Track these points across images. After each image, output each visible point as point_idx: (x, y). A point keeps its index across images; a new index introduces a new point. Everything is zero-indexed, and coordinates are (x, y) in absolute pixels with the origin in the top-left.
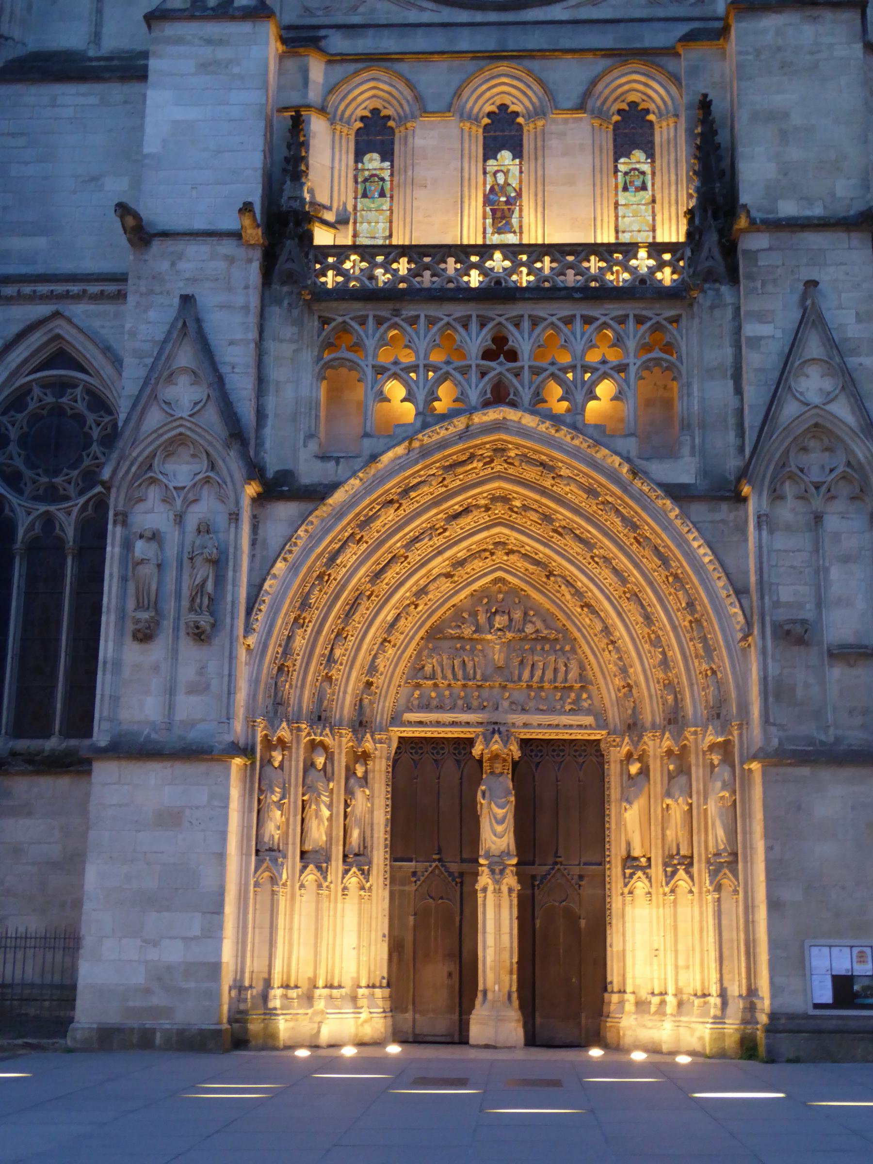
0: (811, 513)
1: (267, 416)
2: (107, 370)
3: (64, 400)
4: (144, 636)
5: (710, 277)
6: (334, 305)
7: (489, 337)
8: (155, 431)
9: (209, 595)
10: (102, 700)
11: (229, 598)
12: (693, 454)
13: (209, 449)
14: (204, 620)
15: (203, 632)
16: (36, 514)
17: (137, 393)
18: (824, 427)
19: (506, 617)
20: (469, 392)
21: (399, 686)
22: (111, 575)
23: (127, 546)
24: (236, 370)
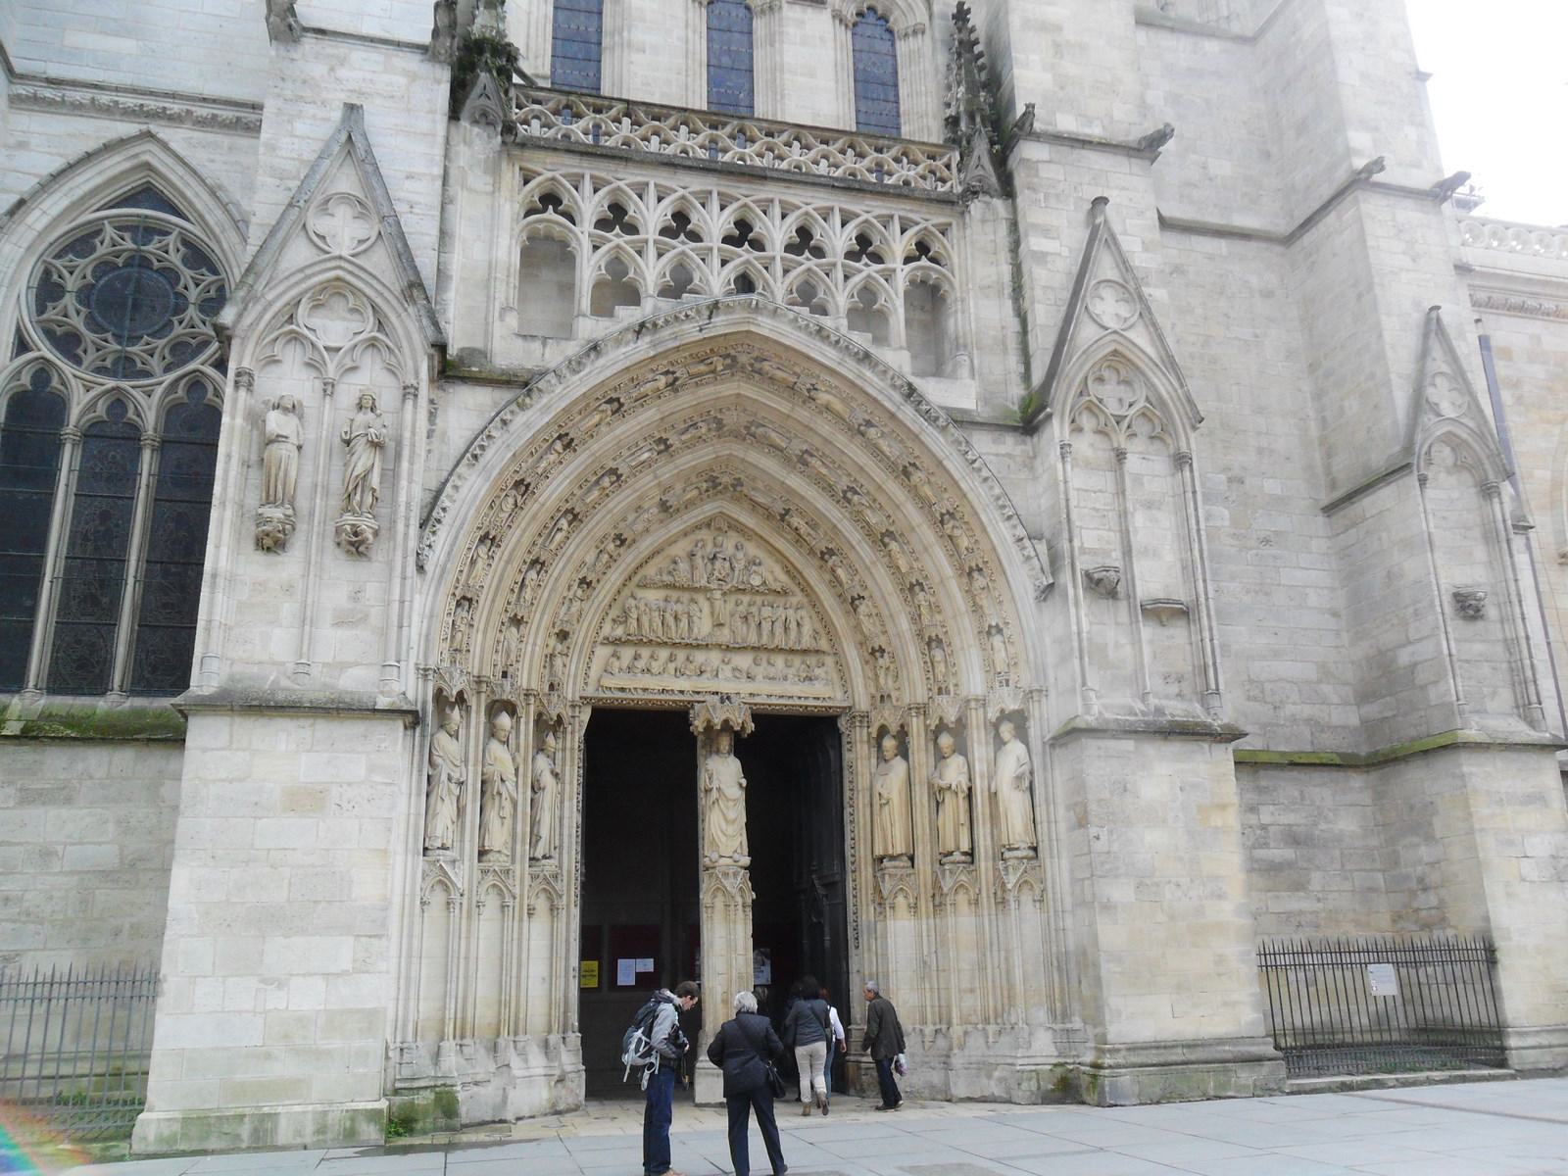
0: (1113, 449)
1: (451, 277)
2: (215, 217)
3: (150, 248)
4: (271, 543)
6: (540, 155)
7: (732, 220)
8: (301, 270)
9: (374, 490)
10: (208, 630)
11: (402, 498)
12: (973, 376)
13: (379, 301)
14: (366, 525)
15: (362, 542)
16: (100, 389)
17: (274, 223)
18: (1124, 356)
19: (727, 564)
20: (711, 278)
21: (595, 642)
22: (229, 456)
23: (256, 420)
24: (415, 210)
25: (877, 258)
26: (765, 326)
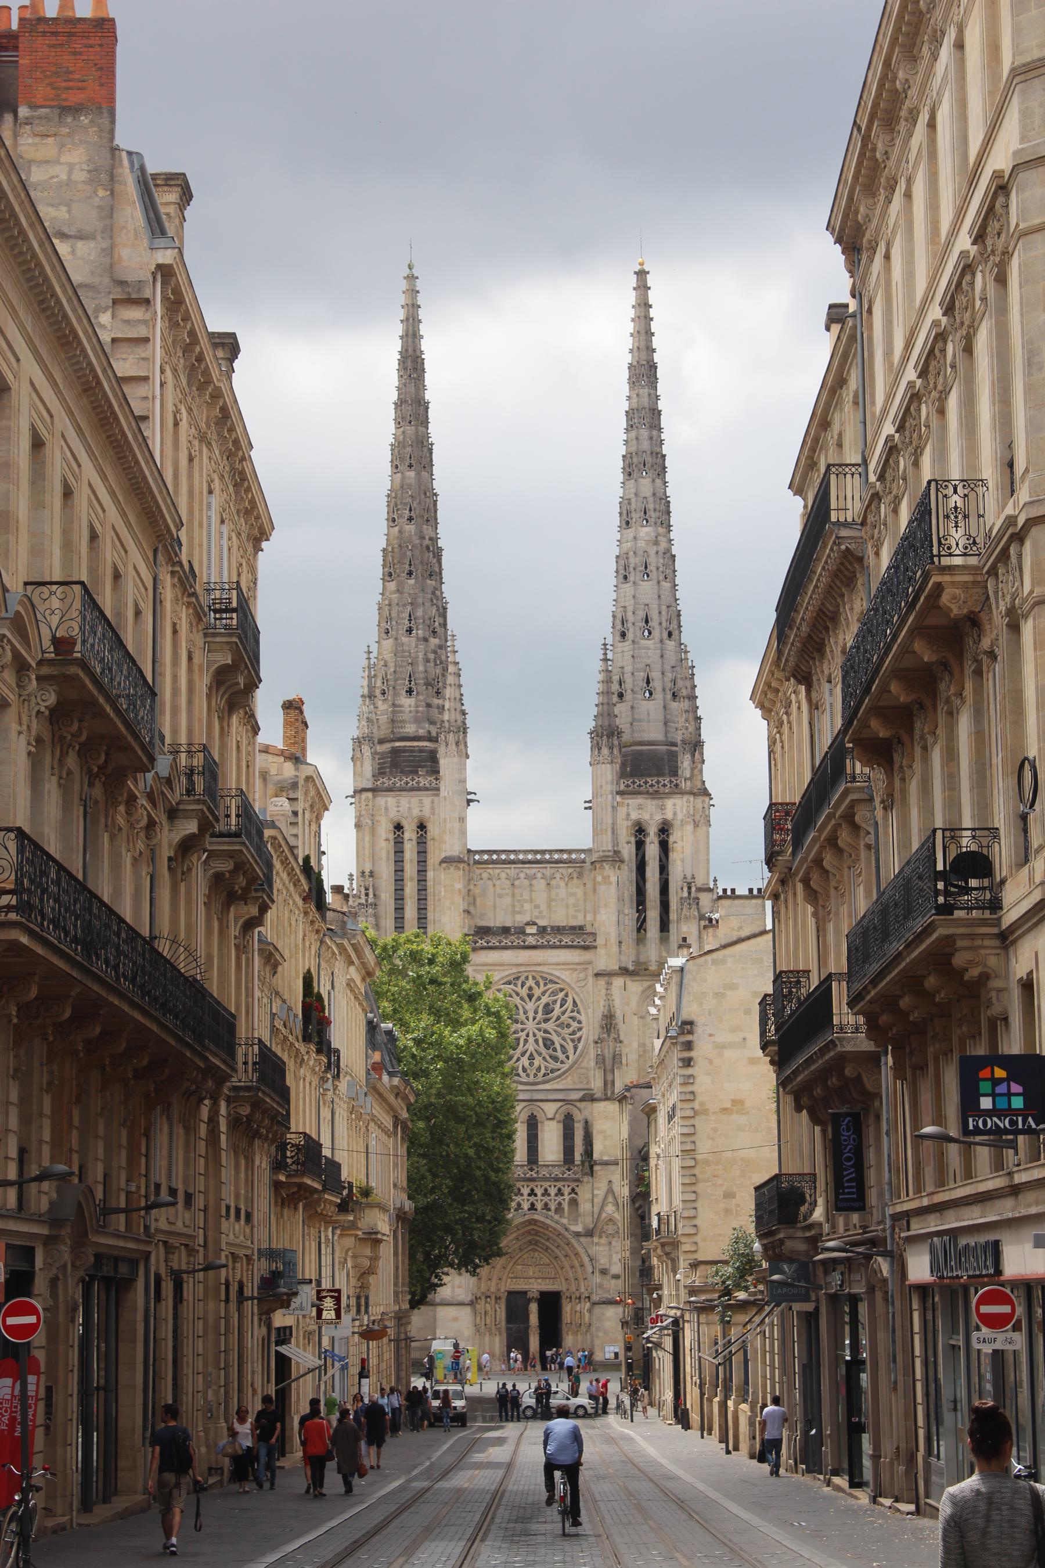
5: (586, 1174)
25: (563, 1195)
26: (536, 1217)
